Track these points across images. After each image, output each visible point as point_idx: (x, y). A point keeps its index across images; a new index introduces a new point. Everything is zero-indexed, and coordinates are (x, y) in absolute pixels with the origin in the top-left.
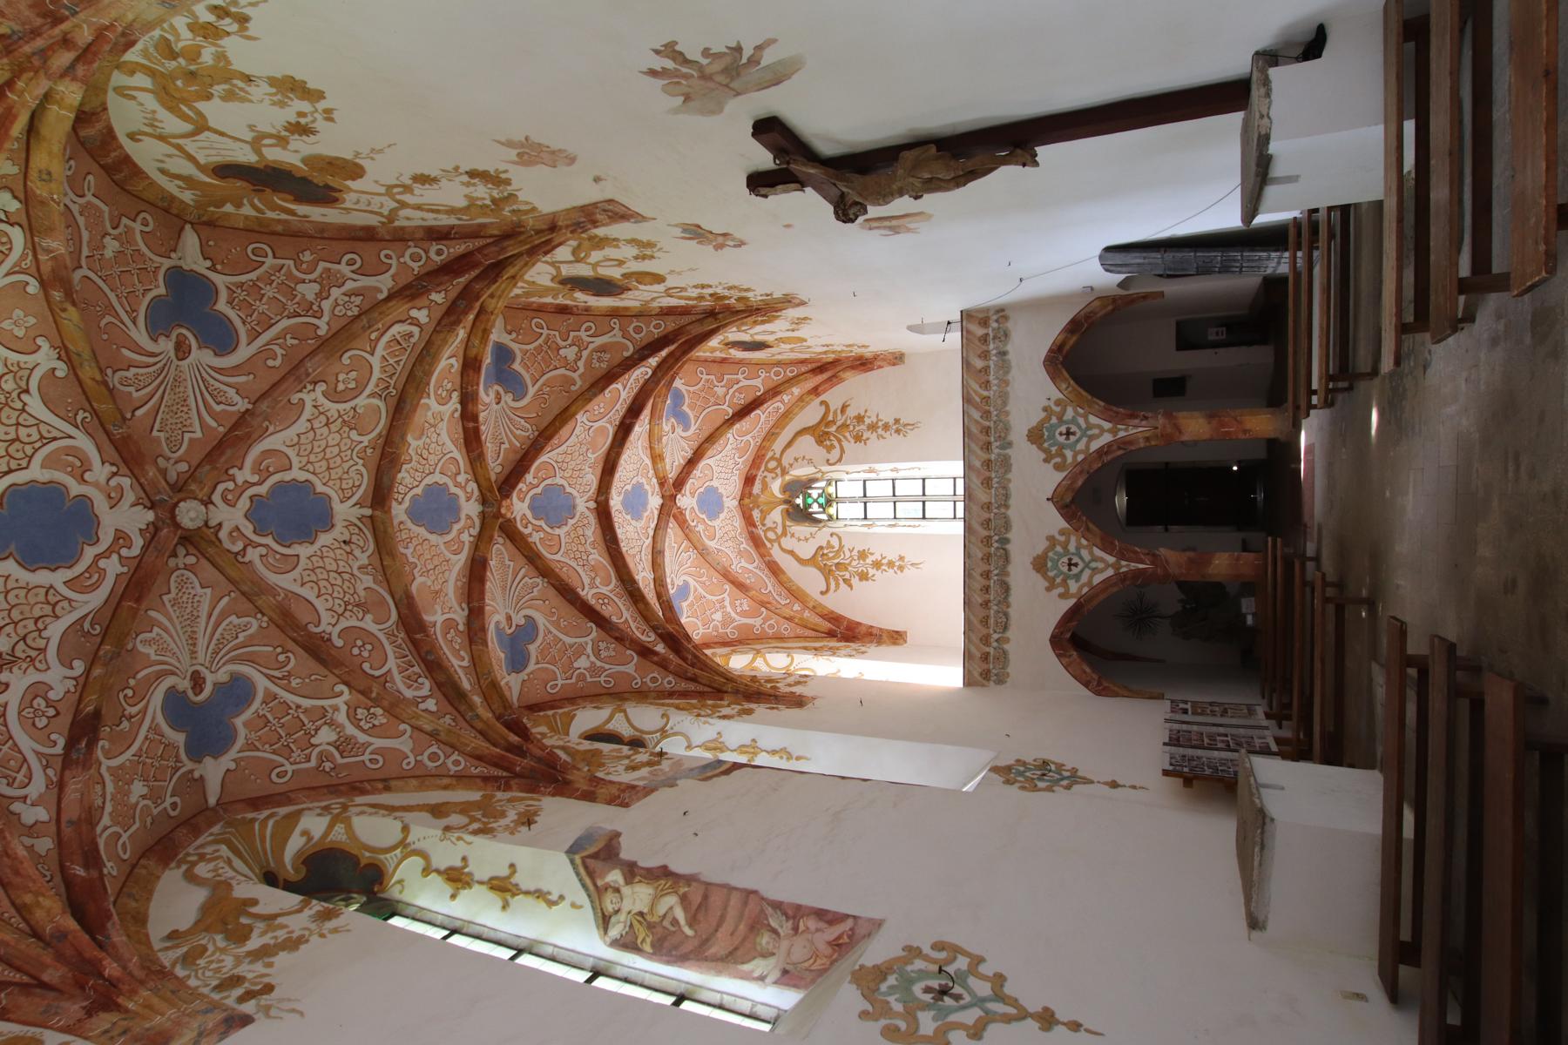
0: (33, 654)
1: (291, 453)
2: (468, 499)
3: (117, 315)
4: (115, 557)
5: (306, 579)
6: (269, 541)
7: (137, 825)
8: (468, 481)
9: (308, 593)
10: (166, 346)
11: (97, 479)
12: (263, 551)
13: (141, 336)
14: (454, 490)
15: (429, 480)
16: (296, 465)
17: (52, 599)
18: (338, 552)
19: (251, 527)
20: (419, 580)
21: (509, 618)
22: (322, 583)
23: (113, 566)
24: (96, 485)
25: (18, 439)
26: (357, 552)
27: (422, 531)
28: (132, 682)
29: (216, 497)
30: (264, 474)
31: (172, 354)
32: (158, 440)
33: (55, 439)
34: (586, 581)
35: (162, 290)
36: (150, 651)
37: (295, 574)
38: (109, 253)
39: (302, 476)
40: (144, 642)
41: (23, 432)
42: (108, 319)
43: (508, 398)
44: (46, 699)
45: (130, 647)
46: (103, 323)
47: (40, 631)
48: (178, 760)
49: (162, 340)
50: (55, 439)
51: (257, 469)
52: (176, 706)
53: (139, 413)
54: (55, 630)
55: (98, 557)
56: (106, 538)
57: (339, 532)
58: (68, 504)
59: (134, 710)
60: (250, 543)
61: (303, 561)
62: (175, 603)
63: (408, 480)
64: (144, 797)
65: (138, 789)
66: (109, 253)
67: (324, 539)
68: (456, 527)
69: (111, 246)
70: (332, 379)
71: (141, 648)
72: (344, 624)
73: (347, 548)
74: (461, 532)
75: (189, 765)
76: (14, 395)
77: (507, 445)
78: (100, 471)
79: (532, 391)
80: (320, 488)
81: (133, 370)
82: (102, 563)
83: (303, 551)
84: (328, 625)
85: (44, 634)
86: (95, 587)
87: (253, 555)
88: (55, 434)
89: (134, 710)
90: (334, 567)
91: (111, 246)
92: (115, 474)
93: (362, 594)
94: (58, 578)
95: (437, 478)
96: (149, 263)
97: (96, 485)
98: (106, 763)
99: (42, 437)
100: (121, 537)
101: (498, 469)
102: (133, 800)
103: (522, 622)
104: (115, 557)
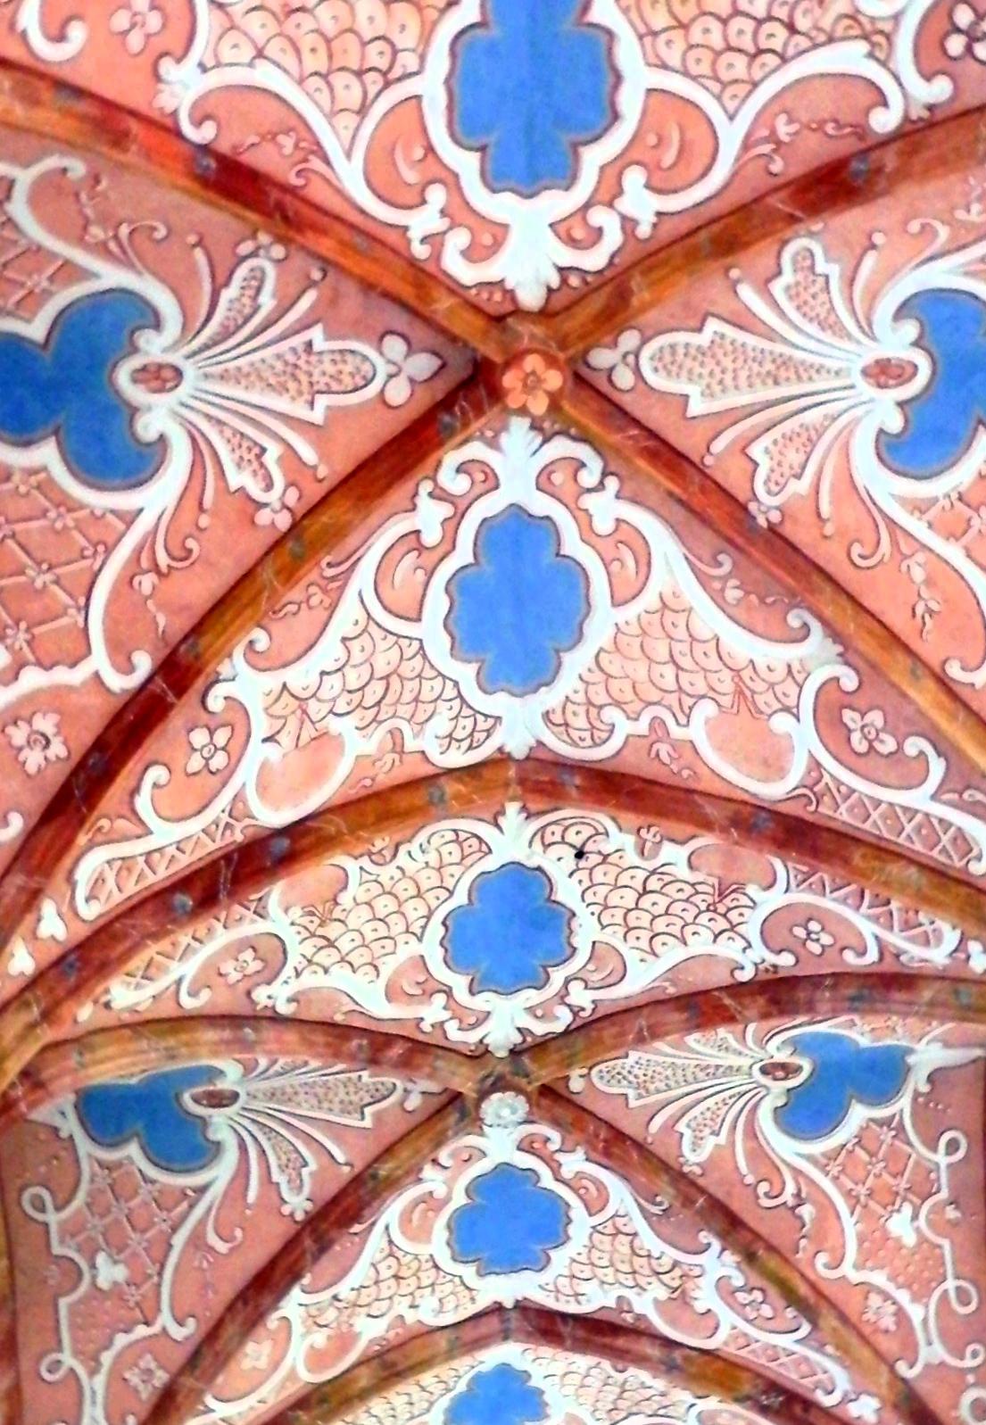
0: (677, 1272)
1: (388, 967)
2: (492, 482)
3: (202, 1222)
4: (560, 1157)
5: (644, 944)
6: (558, 976)
7: (946, 1244)
8: (439, 495)
9: (672, 954)
10: (221, 1124)
11: (446, 1180)
12: (576, 987)
13: (221, 1173)
14: (463, 554)
15: (438, 645)
16: (414, 948)
17: (610, 1230)
18: (598, 876)
19: (532, 992)
20: (697, 732)
21: (884, 373)
22: (660, 925)
23: (575, 1162)
24: (450, 1184)
25: (397, 1277)
26: (607, 848)
27: (576, 662)
28: (750, 1179)
29: (473, 1037)
30: (430, 988)
31: (231, 1110)
32: (378, 1117)
33: (391, 1242)
34: (850, 57)
35: (133, 1150)
36: (710, 1143)
37: (632, 957)
38: (120, 1273)
39: (436, 931)
40: (695, 1147)
41: (386, 1273)
42: (212, 1239)
43: (154, 346)
44: (740, 1289)
45: (698, 1171)
46: (222, 1247)
47: (649, 1256)
48: (885, 1123)
49: (213, 1135)
50: (391, 1242)
51: (428, 995)
52: (809, 1112)
53: (341, 1158)
54: (649, 1241)
55: (558, 1179)
56: (525, 1161)
57: (558, 863)
58: (478, 1200)
59: (790, 1188)
60: (562, 997)
61: (613, 937)
62: (643, 1089)
63: (441, 724)
64: (915, 1217)
65: (902, 1226)
66: (120, 1273)
67: (567, 892)
68: (572, 544)
69: (109, 1272)
70: (242, 987)
71: (703, 1155)
72: (752, 930)
73: (594, 859)
74: (588, 533)
75: (904, 1104)
76: (340, 1305)
77: (316, 334)
78: (433, 1180)
79: (111, 276)
80: (461, 898)
81: (277, 1176)
82: (567, 1173)
83: (586, 932)
84: (748, 956)
85: (656, 1254)
86: (601, 1187)
87: (581, 997)
88: (384, 1244)
89: (790, 1188)
90: (630, 898)
91: (109, 1272)
92: (435, 1161)
93: (699, 877)
94: (581, 1223)
95: (432, 631)
96: (102, 1183)
97: (450, 1184)
98: (848, 1270)
99: (391, 1255)
100: (526, 1146)
101: (395, 346)
102: (910, 1239)
103: (910, 330)
104: (560, 1157)
